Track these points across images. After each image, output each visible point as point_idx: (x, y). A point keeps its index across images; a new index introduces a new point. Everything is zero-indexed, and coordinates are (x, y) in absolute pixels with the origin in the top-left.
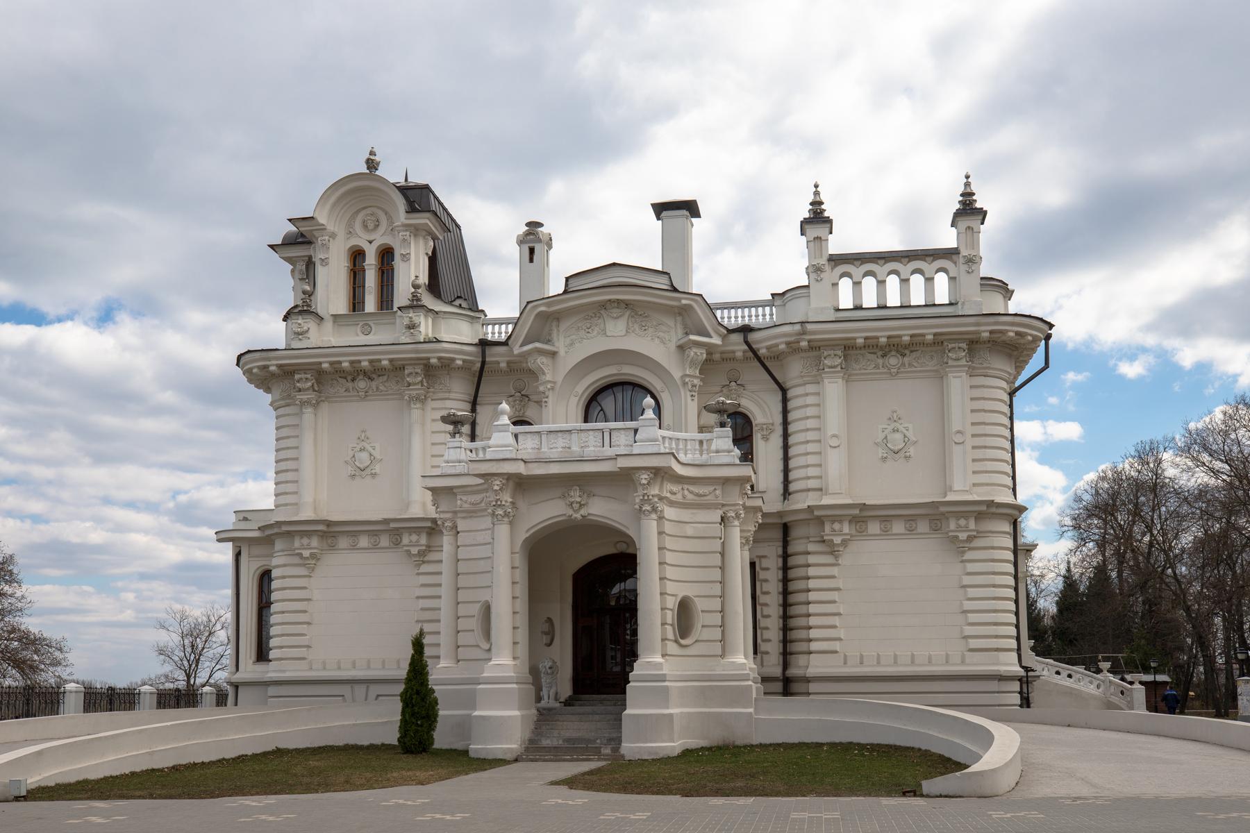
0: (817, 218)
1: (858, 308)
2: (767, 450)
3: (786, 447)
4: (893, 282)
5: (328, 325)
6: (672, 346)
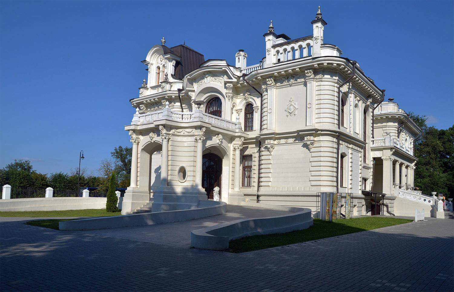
2: (256, 116)
3: (261, 114)
5: (150, 89)
6: (223, 84)
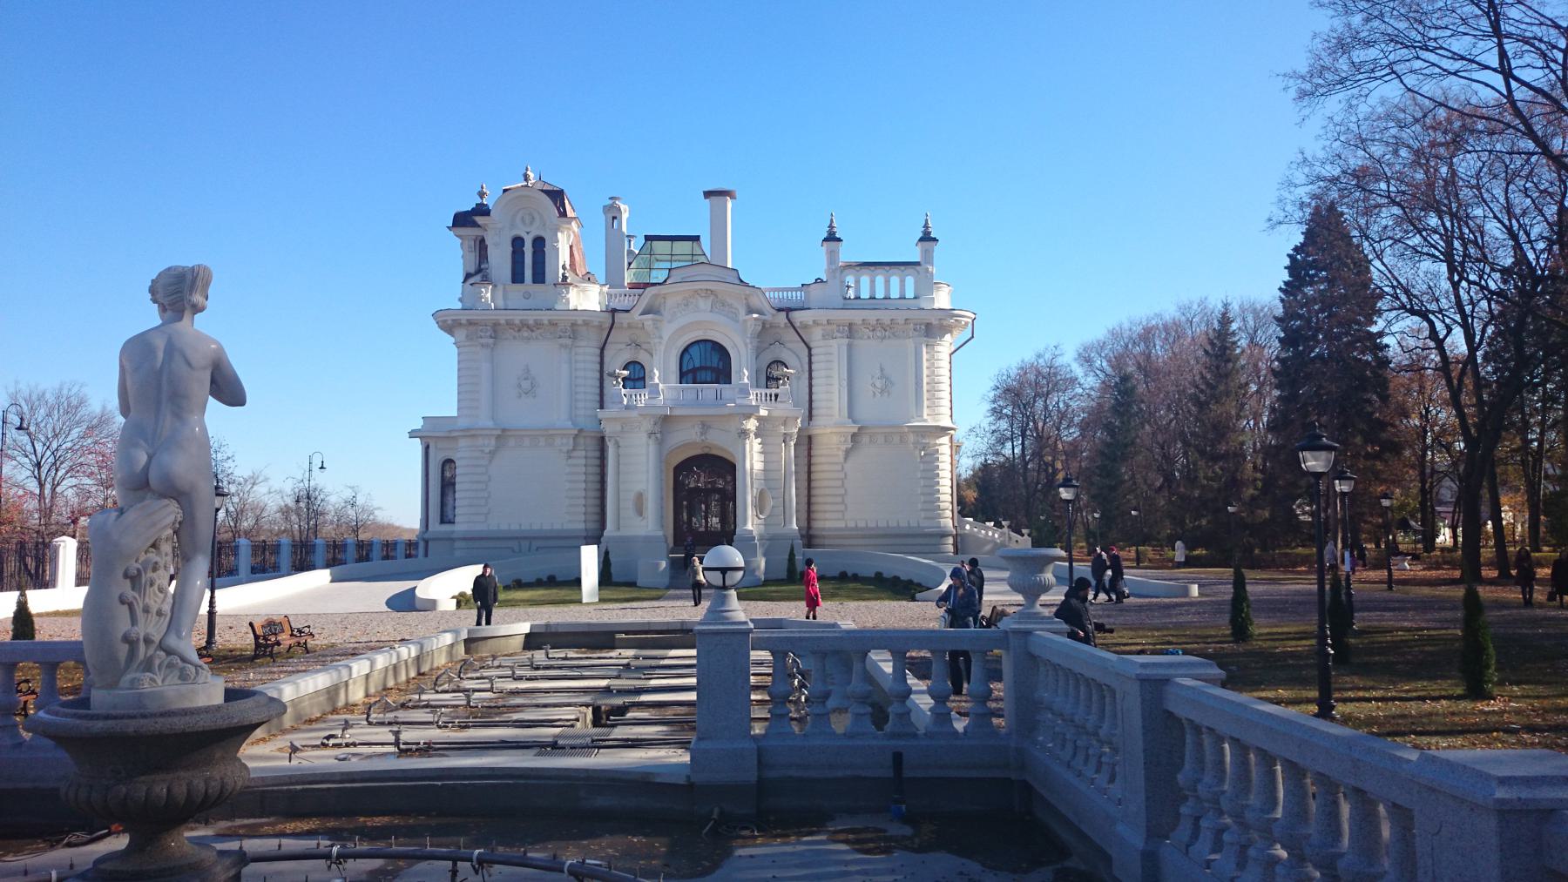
0: (832, 238)
1: (858, 298)
4: (880, 280)
